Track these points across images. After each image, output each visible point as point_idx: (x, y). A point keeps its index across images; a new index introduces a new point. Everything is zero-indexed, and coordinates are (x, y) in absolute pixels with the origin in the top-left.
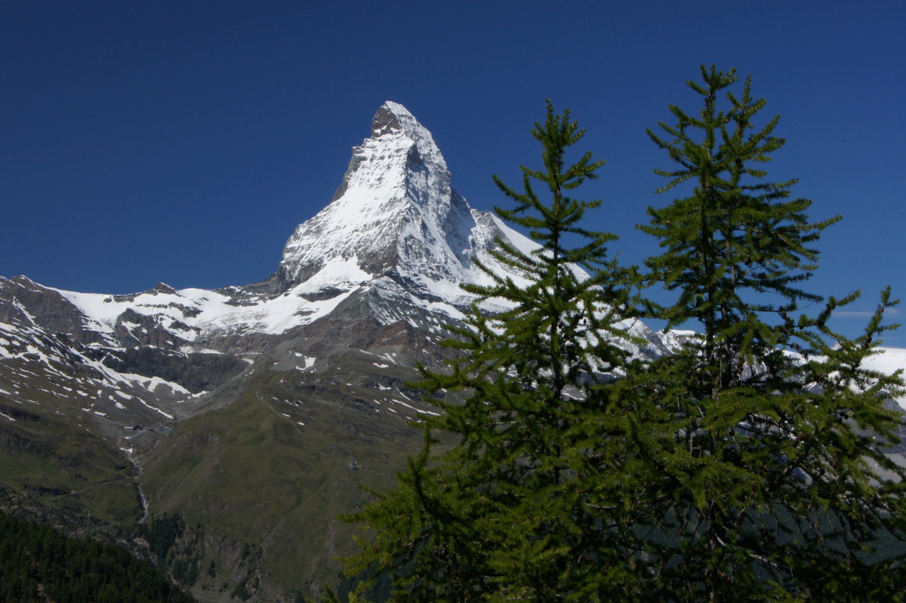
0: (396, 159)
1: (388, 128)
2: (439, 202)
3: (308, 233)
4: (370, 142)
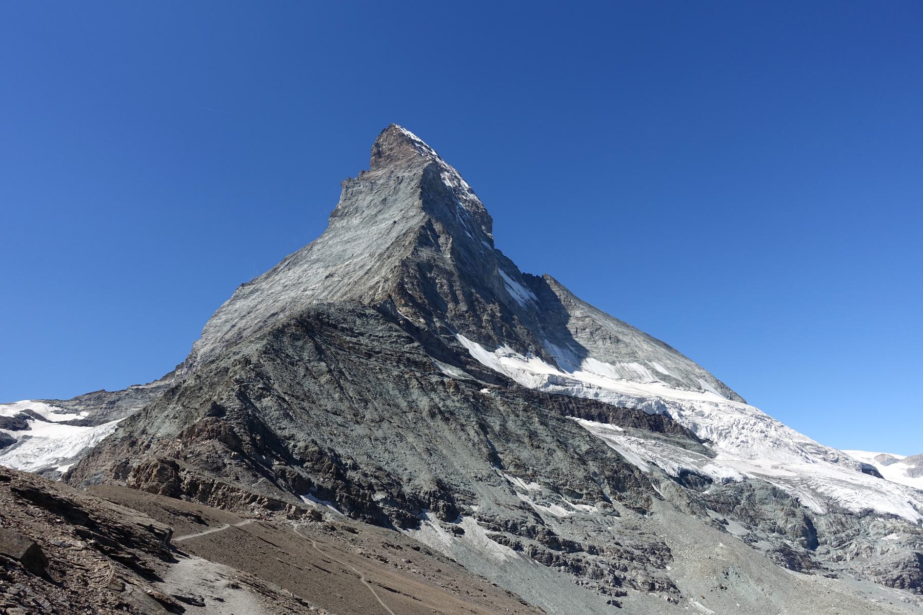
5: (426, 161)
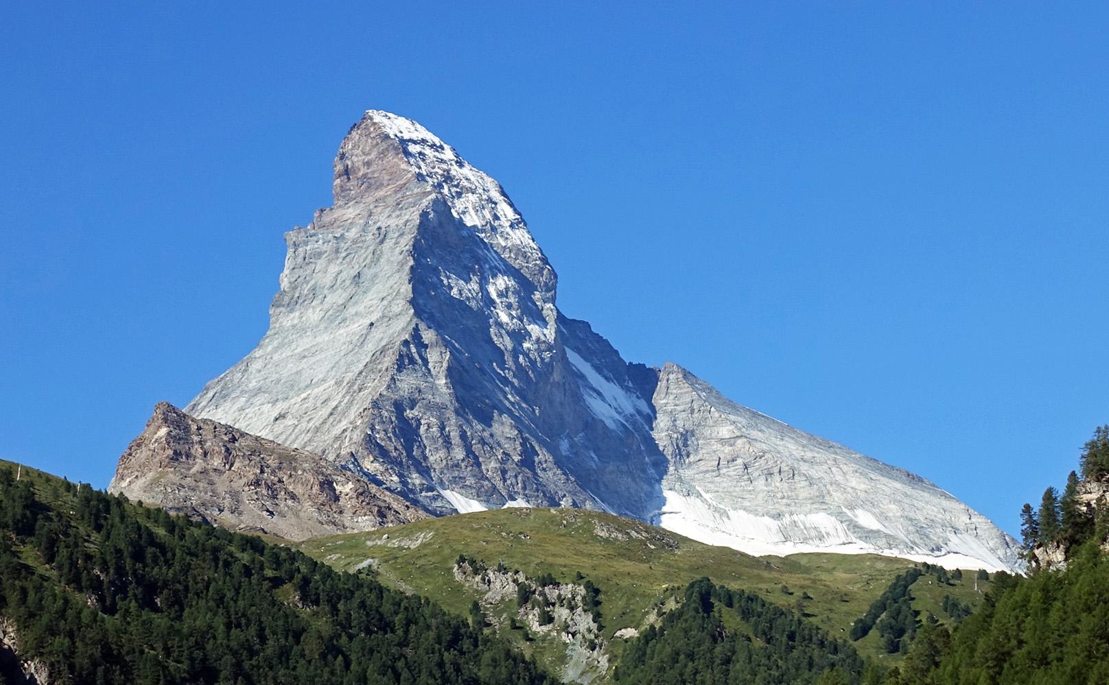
5: (427, 194)
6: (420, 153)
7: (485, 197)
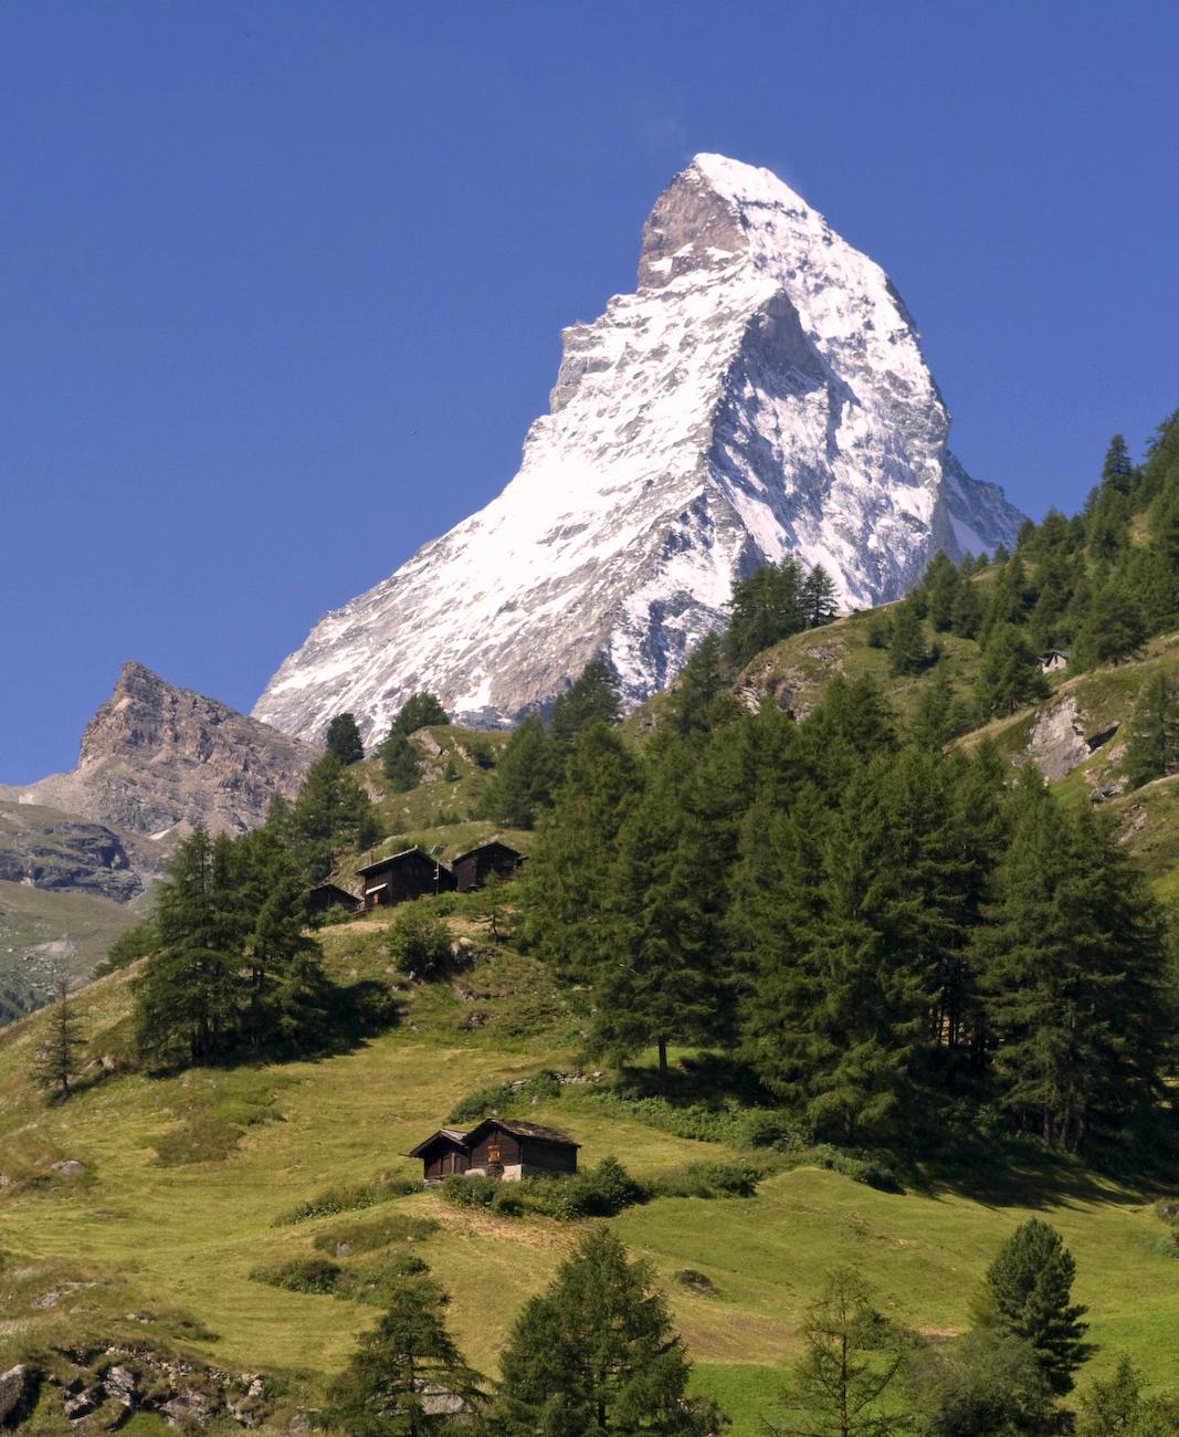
0: (704, 351)
1: (696, 248)
2: (873, 508)
3: (351, 637)
4: (628, 307)
6: (769, 224)
7: (859, 293)
